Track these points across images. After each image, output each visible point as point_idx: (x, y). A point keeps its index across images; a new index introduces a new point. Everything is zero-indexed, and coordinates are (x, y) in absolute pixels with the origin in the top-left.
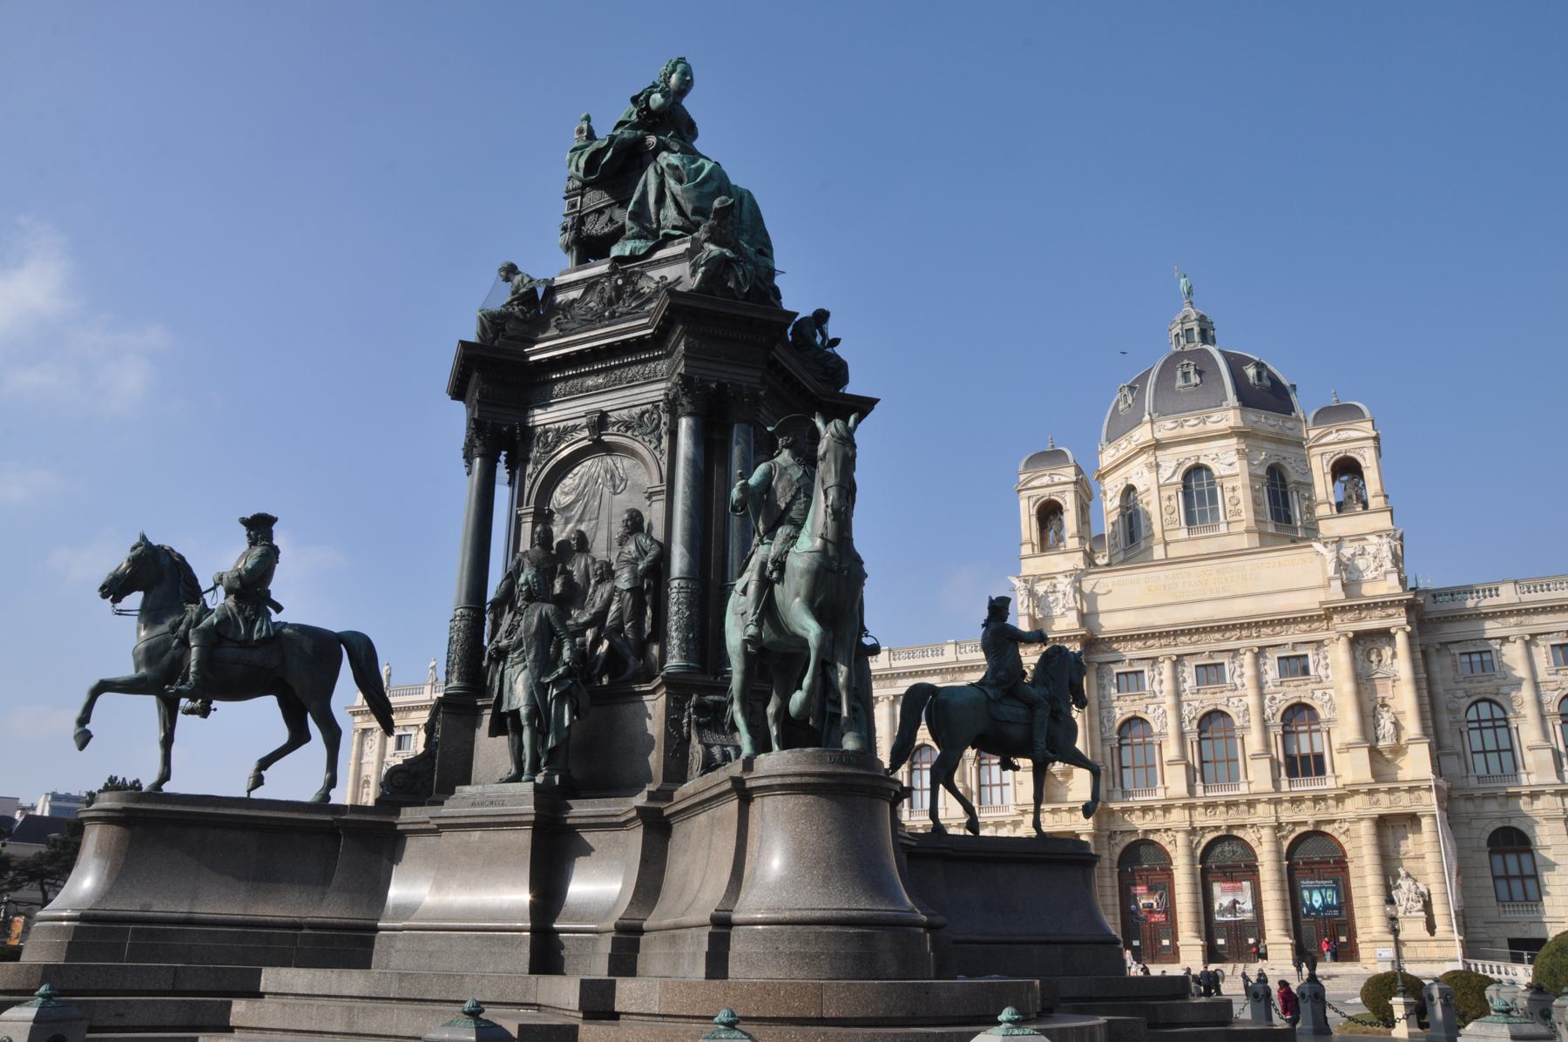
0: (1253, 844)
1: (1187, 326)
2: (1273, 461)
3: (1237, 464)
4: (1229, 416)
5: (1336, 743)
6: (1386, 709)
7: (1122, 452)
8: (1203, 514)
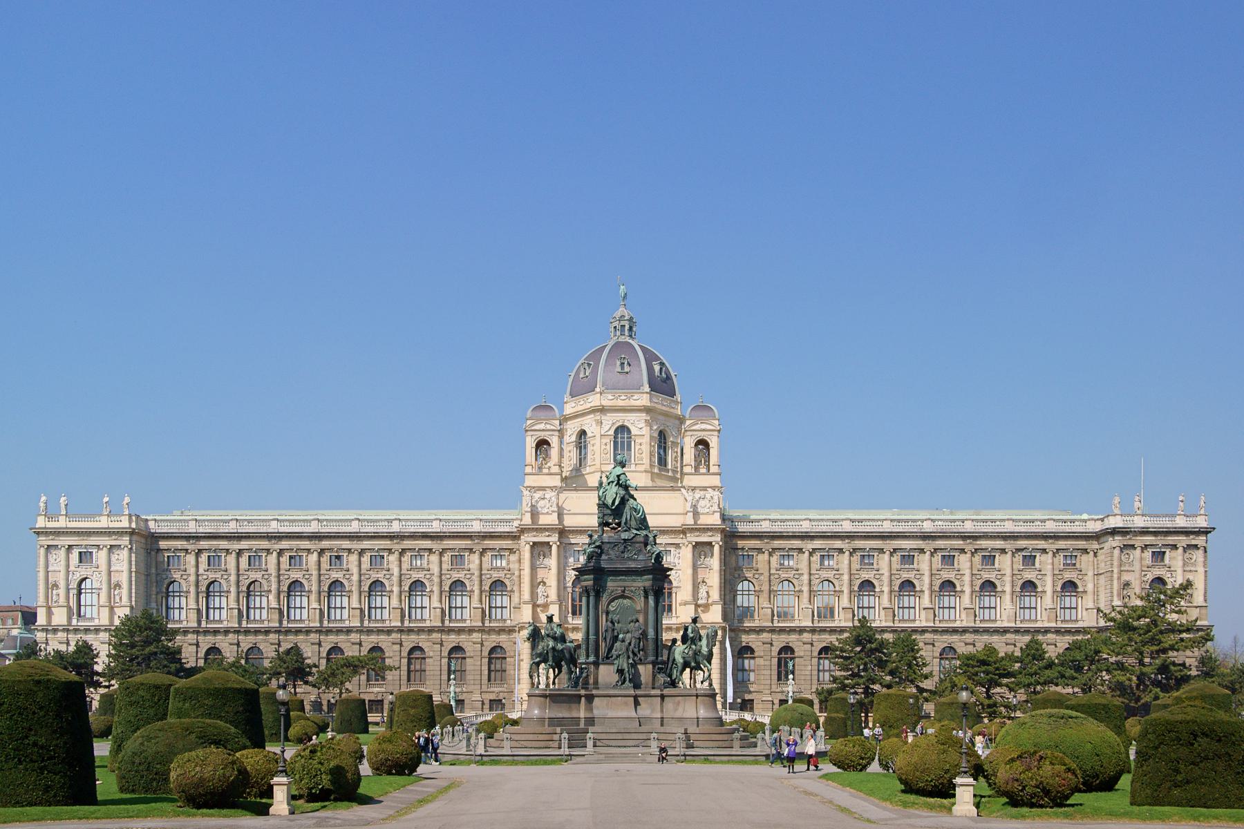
1: (622, 323)
2: (661, 428)
3: (644, 429)
4: (643, 399)
7: (580, 408)
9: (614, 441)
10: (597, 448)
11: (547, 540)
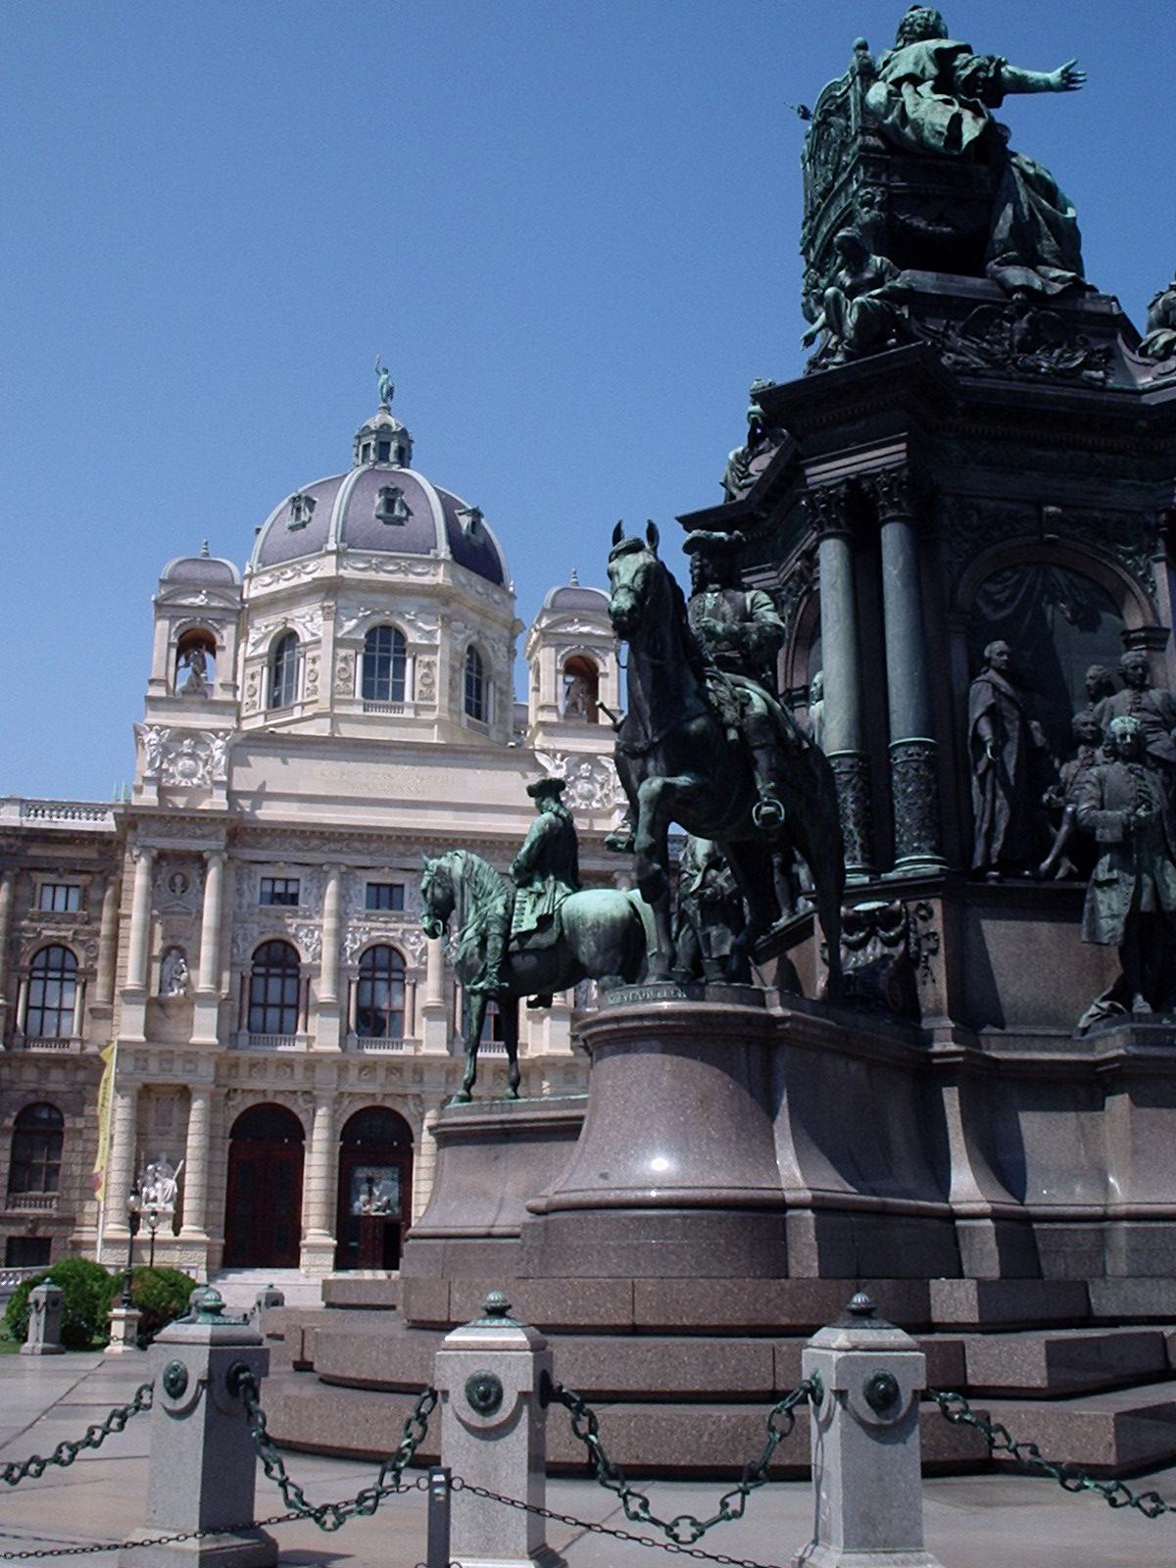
0: (410, 1121)
2: (475, 638)
7: (283, 585)
8: (384, 687)
9: (365, 658)
10: (324, 667)
11: (196, 845)
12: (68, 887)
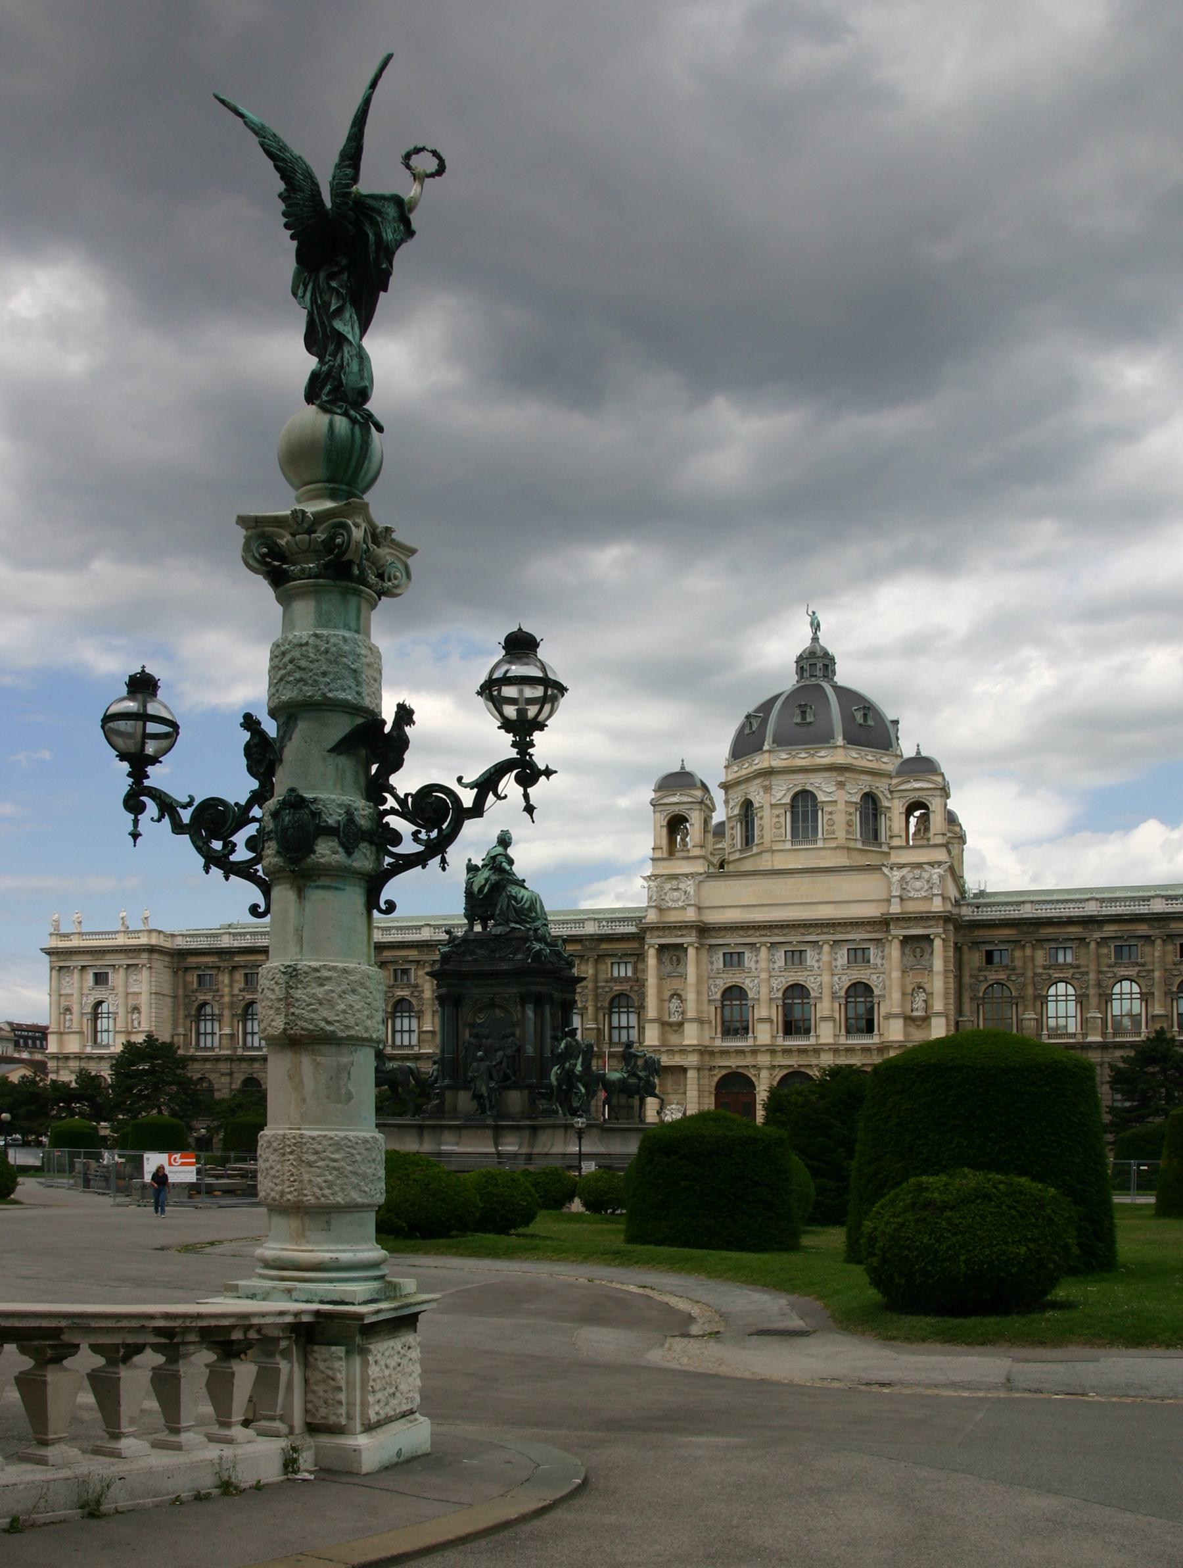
5: (882, 1013)
6: (921, 990)
7: (744, 772)
8: (805, 829)
9: (792, 812)
12: (626, 963)
